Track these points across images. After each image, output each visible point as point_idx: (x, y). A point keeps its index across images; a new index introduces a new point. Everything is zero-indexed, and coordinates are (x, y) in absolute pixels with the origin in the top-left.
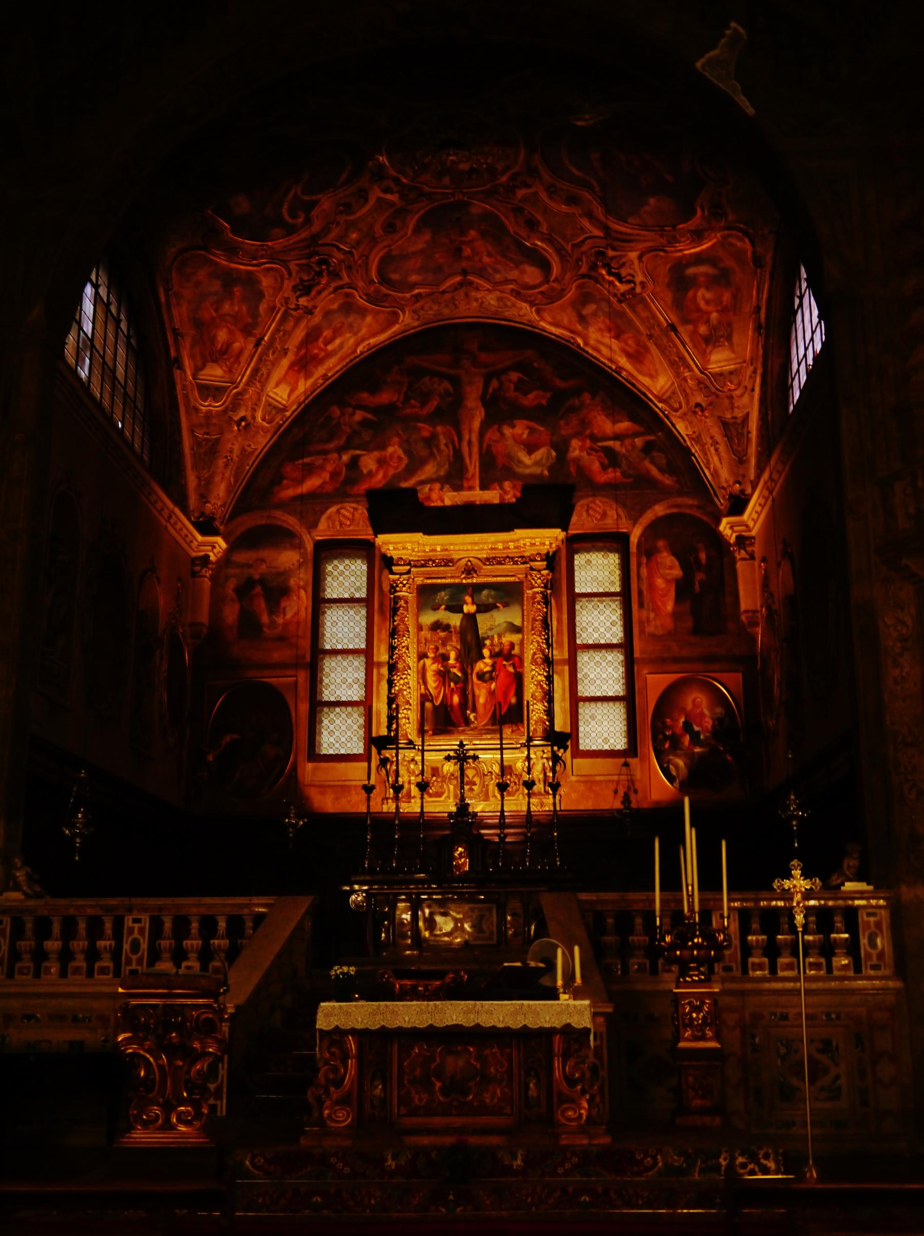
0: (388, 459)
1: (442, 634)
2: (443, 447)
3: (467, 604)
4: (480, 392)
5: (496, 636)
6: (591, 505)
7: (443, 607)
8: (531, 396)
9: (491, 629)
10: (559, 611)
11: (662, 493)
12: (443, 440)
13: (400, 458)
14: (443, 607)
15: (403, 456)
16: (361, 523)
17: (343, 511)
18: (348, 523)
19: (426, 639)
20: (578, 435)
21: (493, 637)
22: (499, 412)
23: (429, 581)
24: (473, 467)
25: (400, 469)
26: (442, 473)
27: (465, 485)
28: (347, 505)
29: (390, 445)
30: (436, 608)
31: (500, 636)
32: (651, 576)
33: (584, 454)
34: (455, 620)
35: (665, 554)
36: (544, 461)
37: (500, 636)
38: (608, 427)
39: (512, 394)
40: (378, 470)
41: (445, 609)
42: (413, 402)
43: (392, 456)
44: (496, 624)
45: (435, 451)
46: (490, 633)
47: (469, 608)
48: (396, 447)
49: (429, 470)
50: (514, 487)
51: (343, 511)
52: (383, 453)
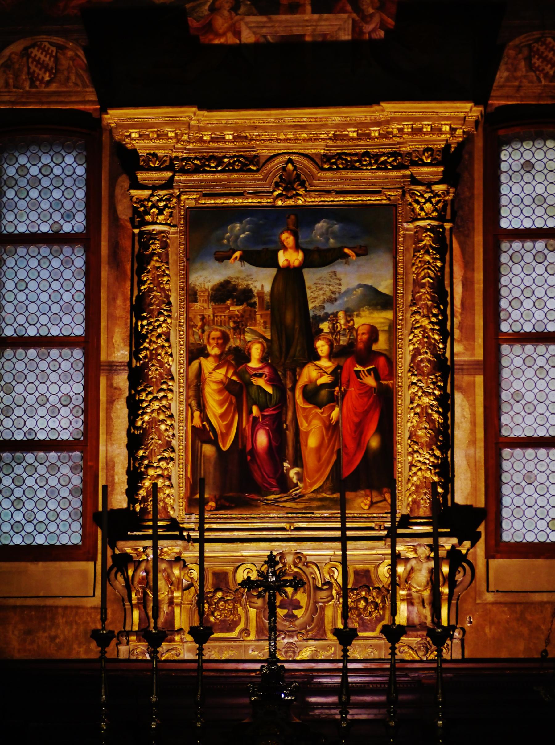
1: (236, 309)
3: (285, 248)
5: (341, 314)
7: (238, 254)
9: (332, 300)
10: (468, 265)
14: (238, 254)
16: (73, 77)
17: (35, 52)
18: (47, 78)
19: (203, 318)
21: (335, 315)
30: (223, 257)
31: (349, 314)
34: (262, 281)
37: (349, 314)
41: (242, 259)
44: (343, 289)
46: (330, 309)
47: (289, 257)
51: (35, 52)
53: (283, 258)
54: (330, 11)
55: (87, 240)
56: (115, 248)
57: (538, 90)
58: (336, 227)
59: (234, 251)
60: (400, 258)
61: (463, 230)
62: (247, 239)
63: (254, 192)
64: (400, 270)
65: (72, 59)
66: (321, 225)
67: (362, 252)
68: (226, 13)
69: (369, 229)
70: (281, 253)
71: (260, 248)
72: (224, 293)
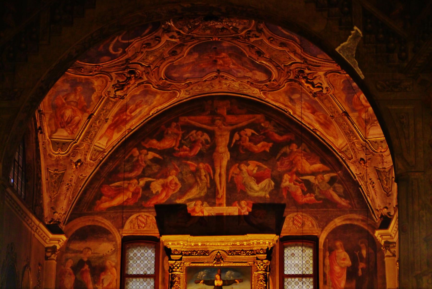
0: (168, 184)
2: (203, 177)
3: (217, 280)
4: (228, 142)
6: (295, 217)
7: (202, 281)
8: (259, 145)
11: (342, 210)
12: (203, 173)
13: (176, 184)
14: (202, 281)
15: (178, 182)
16: (151, 226)
17: (140, 218)
20: (289, 171)
22: (239, 154)
23: (194, 265)
24: (222, 191)
25: (177, 191)
26: (202, 194)
27: (217, 203)
28: (143, 214)
29: (170, 175)
32: (331, 265)
33: (292, 184)
35: (341, 250)
36: (266, 188)
38: (308, 167)
40: (162, 191)
41: (203, 283)
42: (185, 147)
43: (171, 181)
45: (198, 180)
48: (174, 176)
49: (194, 192)
50: (248, 205)
51: (140, 218)
52: (165, 180)
53: (216, 283)
54: (231, 206)
55: (155, 277)
56: (164, 279)
57: (296, 231)
58: (233, 273)
59: (201, 280)
60: (253, 283)
61: (273, 274)
62: (205, 276)
63: (207, 262)
64: (253, 287)
65: (151, 220)
66: (228, 273)
67: (241, 281)
68: (199, 206)
70: (215, 281)
71: (209, 279)
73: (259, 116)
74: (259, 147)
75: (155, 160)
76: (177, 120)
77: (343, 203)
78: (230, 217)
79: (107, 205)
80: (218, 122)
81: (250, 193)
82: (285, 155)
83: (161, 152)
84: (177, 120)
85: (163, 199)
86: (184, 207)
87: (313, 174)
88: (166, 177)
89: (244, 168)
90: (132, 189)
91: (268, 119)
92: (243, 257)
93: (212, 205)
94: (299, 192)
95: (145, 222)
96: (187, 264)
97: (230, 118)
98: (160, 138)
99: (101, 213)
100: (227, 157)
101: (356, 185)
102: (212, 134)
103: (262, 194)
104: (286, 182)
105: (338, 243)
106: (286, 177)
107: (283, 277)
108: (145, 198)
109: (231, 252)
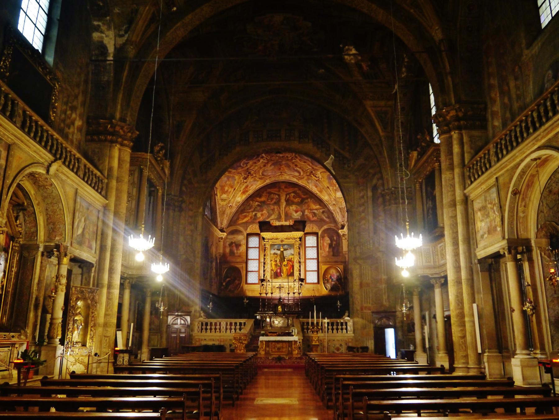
12: (276, 210)
20: (308, 209)
22: (289, 202)
24: (283, 216)
34: (279, 252)
39: (292, 199)
47: (282, 250)
49: (273, 217)
55: (259, 248)
61: (302, 247)
63: (278, 242)
69: (291, 246)
72: (274, 254)
73: (296, 189)
74: (296, 200)
75: (258, 205)
76: (266, 190)
77: (327, 220)
78: (286, 226)
79: (241, 222)
80: (281, 191)
81: (294, 217)
82: (306, 203)
83: (261, 202)
84: (266, 190)
85: (261, 219)
86: (269, 222)
87: (316, 210)
88: (262, 211)
89: (291, 208)
90: (250, 216)
91: (300, 190)
92: (291, 240)
93: (279, 221)
94: (311, 216)
95: (255, 228)
96: (271, 243)
97: (286, 190)
98: (260, 197)
99: (239, 225)
100: (284, 204)
101: (332, 214)
102: (279, 195)
103: (297, 217)
104: (307, 212)
105: (326, 235)
106: (306, 211)
107: (305, 247)
108: (255, 219)
109: (286, 239)
